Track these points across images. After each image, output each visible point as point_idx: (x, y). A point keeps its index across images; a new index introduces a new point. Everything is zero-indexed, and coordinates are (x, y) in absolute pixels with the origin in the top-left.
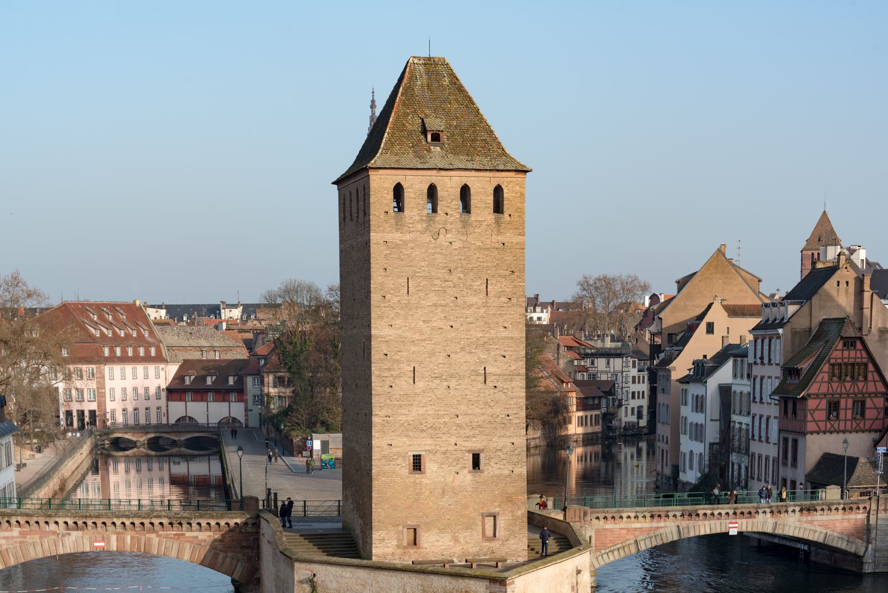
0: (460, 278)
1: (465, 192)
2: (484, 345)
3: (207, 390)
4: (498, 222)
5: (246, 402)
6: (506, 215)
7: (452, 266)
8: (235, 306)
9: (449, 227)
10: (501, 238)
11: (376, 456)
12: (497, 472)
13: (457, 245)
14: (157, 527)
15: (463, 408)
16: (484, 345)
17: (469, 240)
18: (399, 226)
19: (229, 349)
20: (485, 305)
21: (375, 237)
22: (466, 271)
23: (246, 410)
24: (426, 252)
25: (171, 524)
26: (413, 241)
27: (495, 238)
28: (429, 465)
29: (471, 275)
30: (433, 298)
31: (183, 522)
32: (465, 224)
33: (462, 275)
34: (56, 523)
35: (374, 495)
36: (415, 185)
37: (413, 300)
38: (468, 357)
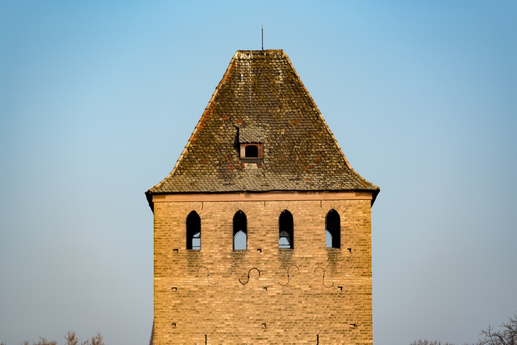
0: (278, 335)
4: (332, 259)
6: (344, 251)
7: (267, 318)
9: (263, 267)
10: (336, 280)
13: (274, 290)
17: (292, 283)
22: (287, 325)
24: (231, 300)
26: (213, 286)
27: (328, 281)
29: (295, 330)
33: (281, 331)
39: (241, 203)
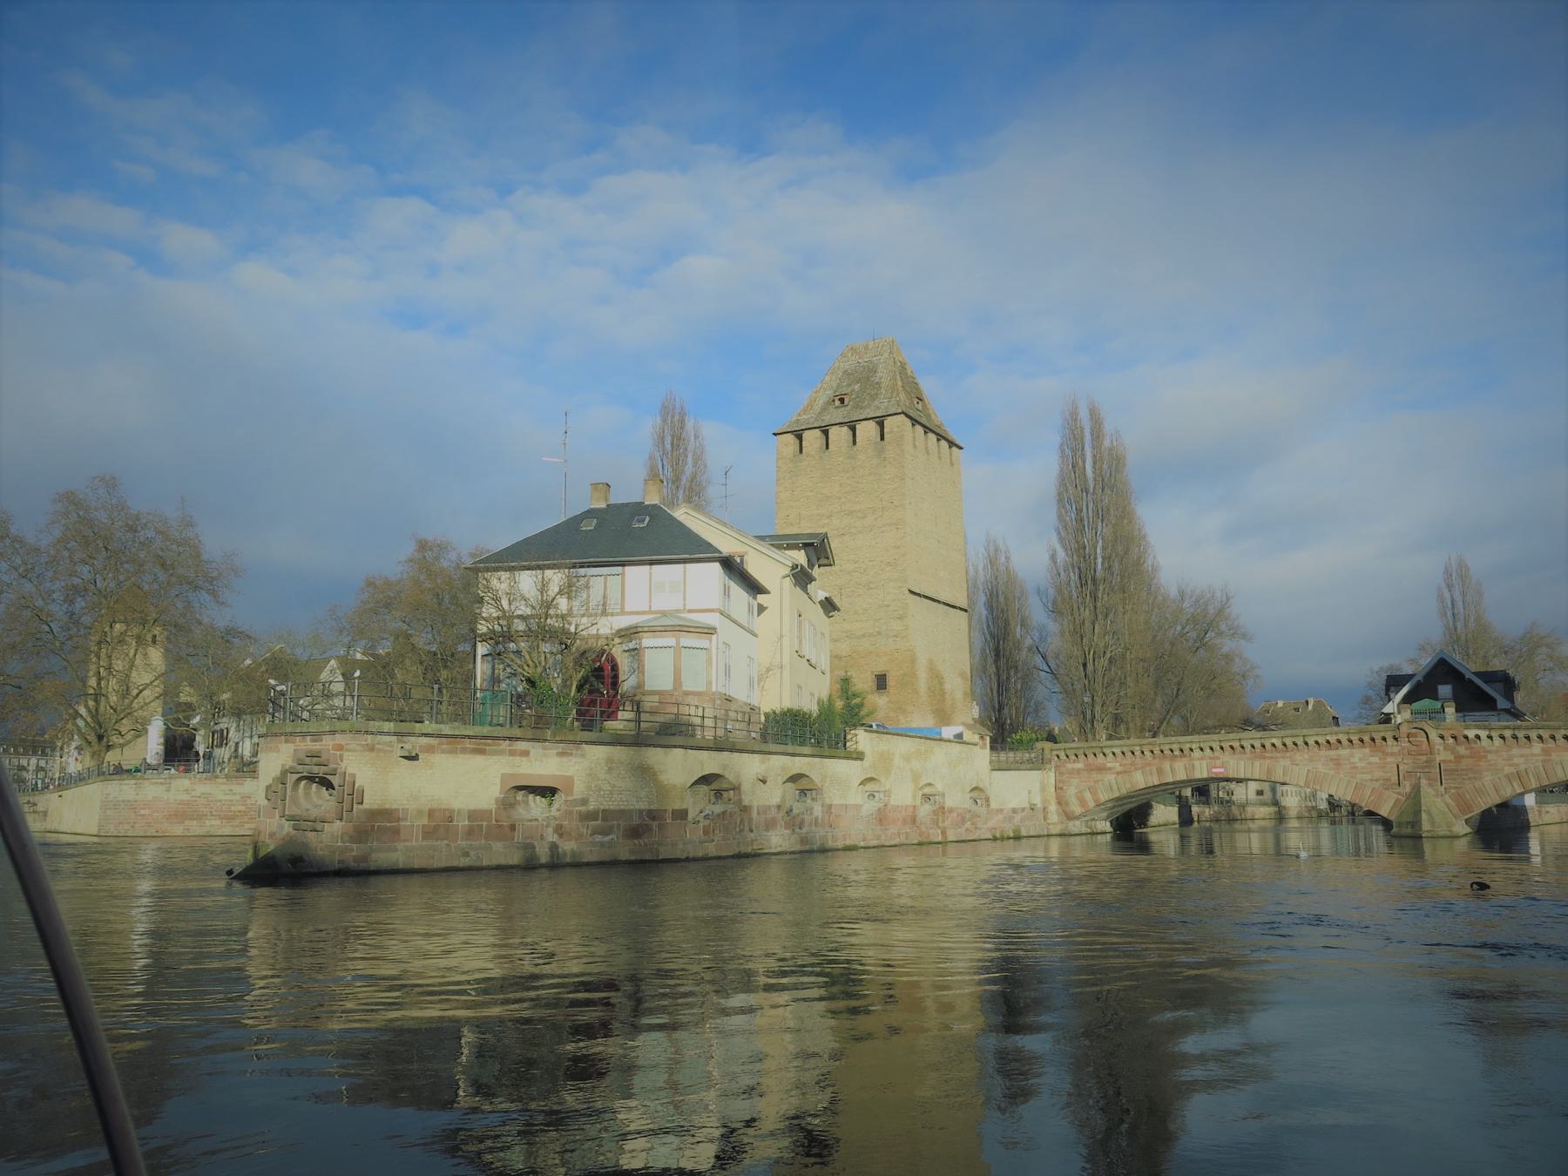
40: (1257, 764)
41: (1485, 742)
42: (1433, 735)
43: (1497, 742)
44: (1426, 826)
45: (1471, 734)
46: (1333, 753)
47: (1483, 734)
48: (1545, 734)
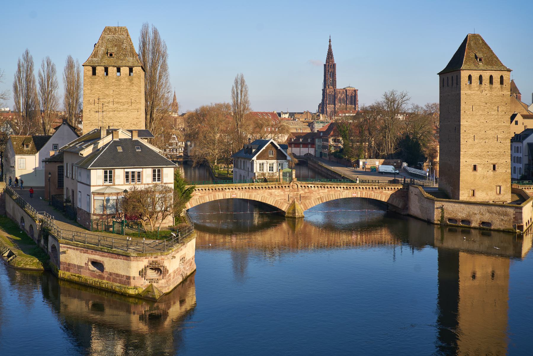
1: (491, 77)
2: (497, 128)
3: (300, 143)
4: (501, 87)
5: (315, 148)
7: (487, 102)
8: (286, 113)
10: (503, 93)
11: (461, 165)
12: (501, 171)
13: (488, 95)
14: (374, 189)
15: (490, 149)
16: (497, 128)
18: (470, 88)
19: (305, 129)
20: (498, 115)
21: (462, 92)
22: (491, 104)
23: (315, 151)
25: (379, 188)
27: (501, 93)
28: (479, 168)
30: (481, 112)
31: (383, 187)
32: (491, 88)
34: (340, 187)
35: (461, 178)
36: (475, 75)
37: (474, 113)
38: (492, 132)
39: (481, 73)
40: (246, 194)
41: (313, 188)
42: (299, 186)
43: (316, 188)
44: (297, 214)
45: (310, 186)
46: (270, 191)
47: (313, 186)
48: (329, 186)
